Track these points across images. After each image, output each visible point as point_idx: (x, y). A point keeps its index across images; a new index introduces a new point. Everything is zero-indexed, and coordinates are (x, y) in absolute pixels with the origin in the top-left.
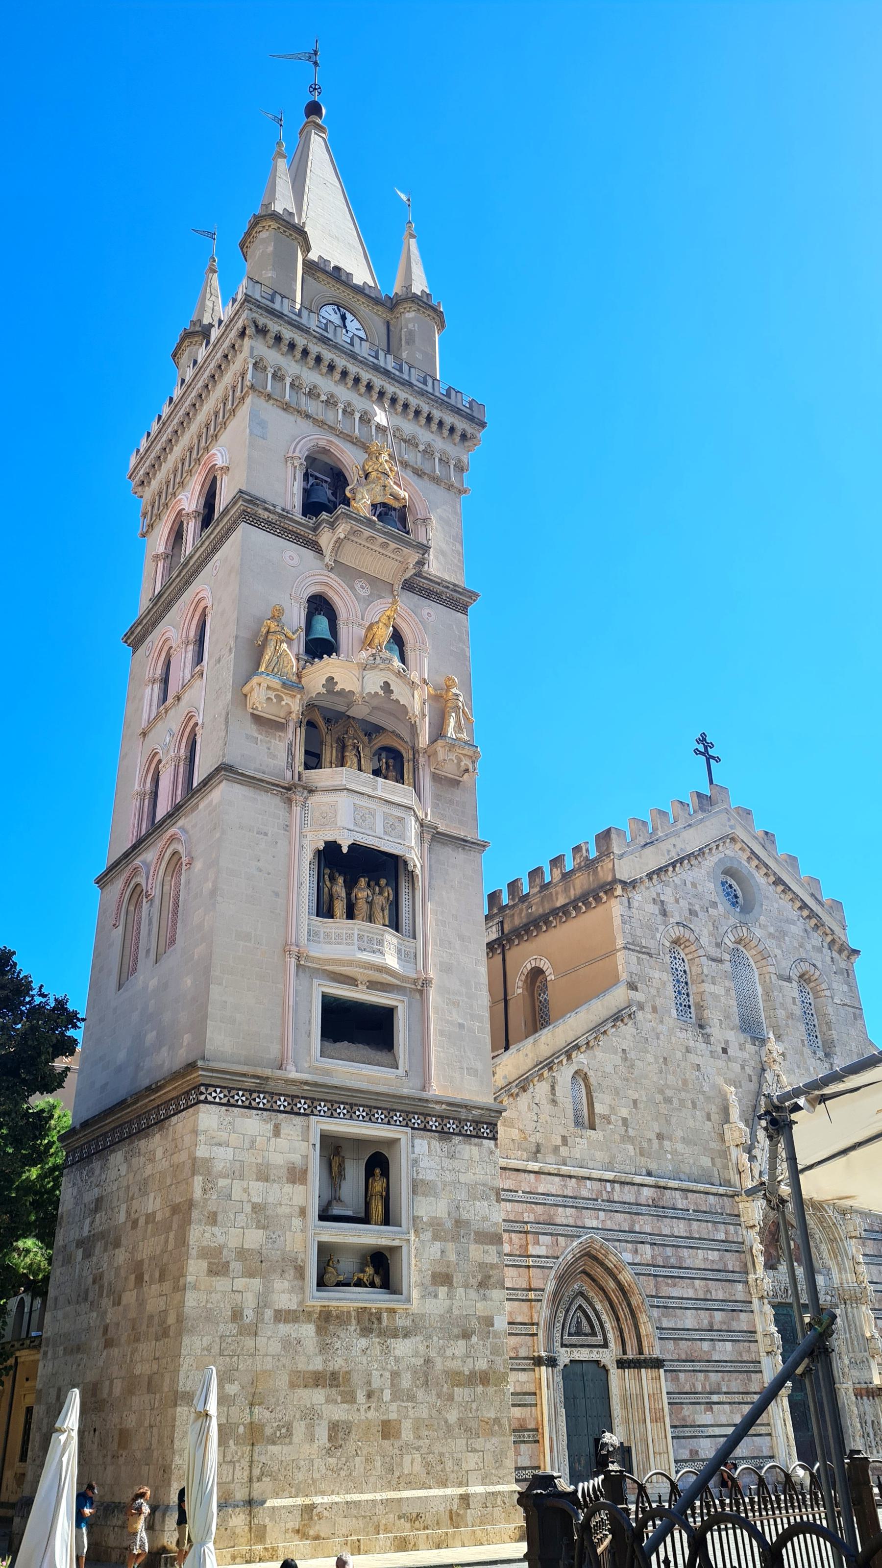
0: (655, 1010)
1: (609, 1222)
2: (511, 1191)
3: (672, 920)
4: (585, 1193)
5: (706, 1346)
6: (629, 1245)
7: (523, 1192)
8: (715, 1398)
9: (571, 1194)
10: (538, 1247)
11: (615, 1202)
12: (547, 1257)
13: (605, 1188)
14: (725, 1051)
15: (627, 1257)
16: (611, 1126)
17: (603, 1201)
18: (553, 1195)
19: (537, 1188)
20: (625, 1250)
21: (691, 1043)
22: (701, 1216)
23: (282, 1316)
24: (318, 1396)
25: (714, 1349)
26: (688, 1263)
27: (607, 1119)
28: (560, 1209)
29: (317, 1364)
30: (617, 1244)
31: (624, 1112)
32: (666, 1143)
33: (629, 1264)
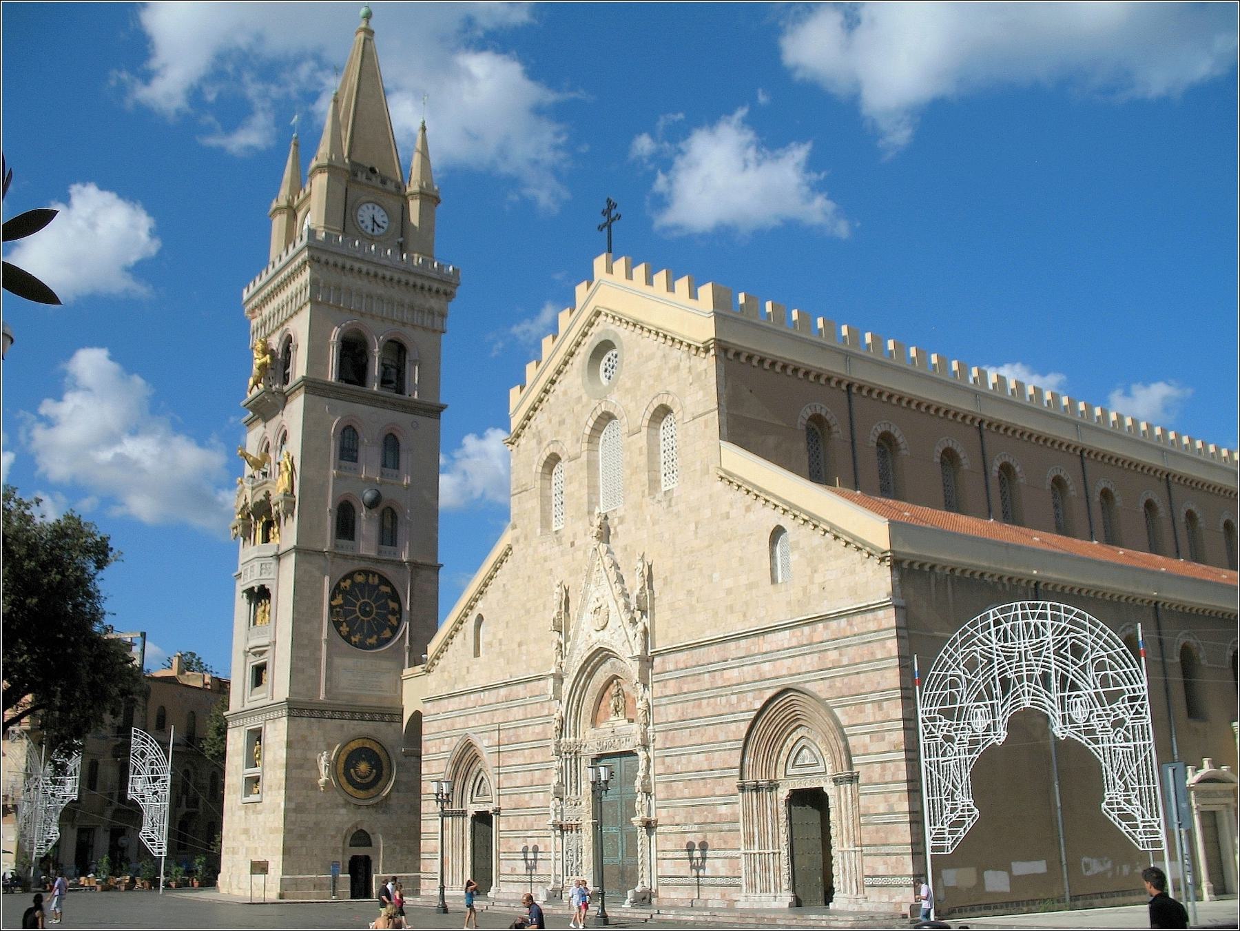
0: (526, 538)
3: (545, 444)
4: (470, 705)
5: (527, 797)
8: (529, 834)
14: (572, 544)
15: (486, 743)
21: (548, 552)
22: (534, 700)
23: (240, 808)
24: (243, 837)
25: (532, 798)
26: (522, 738)
29: (243, 826)
31: (500, 635)
32: (524, 647)
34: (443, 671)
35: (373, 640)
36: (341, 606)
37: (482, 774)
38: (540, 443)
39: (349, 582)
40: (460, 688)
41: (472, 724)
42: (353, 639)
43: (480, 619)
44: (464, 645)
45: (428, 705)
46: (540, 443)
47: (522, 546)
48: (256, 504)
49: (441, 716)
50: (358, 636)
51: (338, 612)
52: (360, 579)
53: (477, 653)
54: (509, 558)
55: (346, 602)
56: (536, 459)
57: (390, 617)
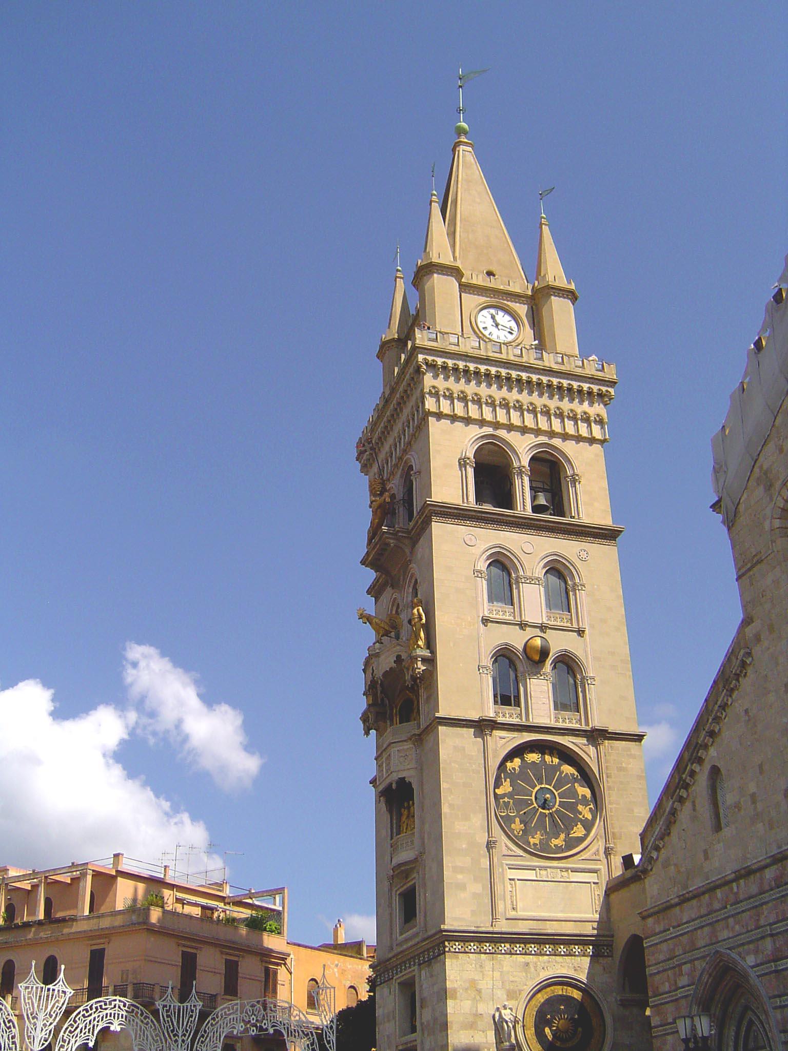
0: (771, 629)
1: (737, 927)
2: (665, 931)
3: (778, 485)
4: (717, 905)
6: (751, 946)
7: (674, 928)
9: (706, 912)
10: (682, 978)
11: (741, 901)
12: (689, 986)
13: (732, 889)
15: (751, 960)
16: (742, 812)
17: (731, 905)
18: (693, 920)
19: (681, 919)
20: (748, 953)
27: (737, 806)
28: (699, 931)
30: (741, 949)
31: (752, 788)
33: (752, 967)
34: (666, 865)
35: (559, 841)
36: (510, 795)
37: (750, 1014)
38: (769, 487)
39: (517, 761)
40: (697, 883)
41: (725, 934)
42: (532, 841)
43: (715, 771)
44: (694, 818)
45: (650, 921)
46: (769, 487)
47: (766, 643)
48: (386, 674)
49: (672, 932)
50: (538, 836)
51: (507, 805)
52: (533, 757)
53: (718, 828)
54: (750, 670)
55: (516, 790)
56: (768, 512)
57: (580, 808)
